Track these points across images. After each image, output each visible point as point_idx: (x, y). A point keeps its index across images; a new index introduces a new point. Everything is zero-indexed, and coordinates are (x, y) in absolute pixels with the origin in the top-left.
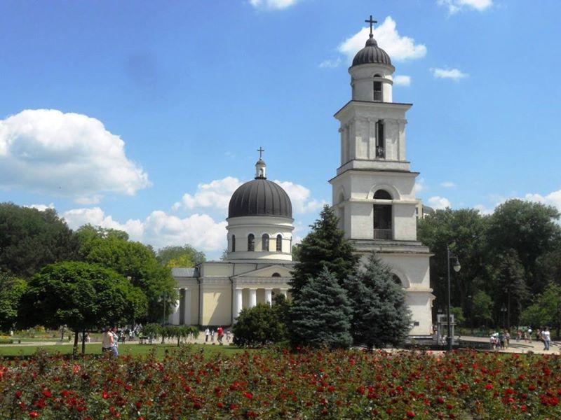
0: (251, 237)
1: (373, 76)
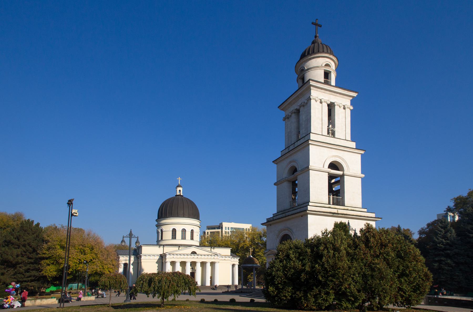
0: (174, 231)
1: (323, 65)
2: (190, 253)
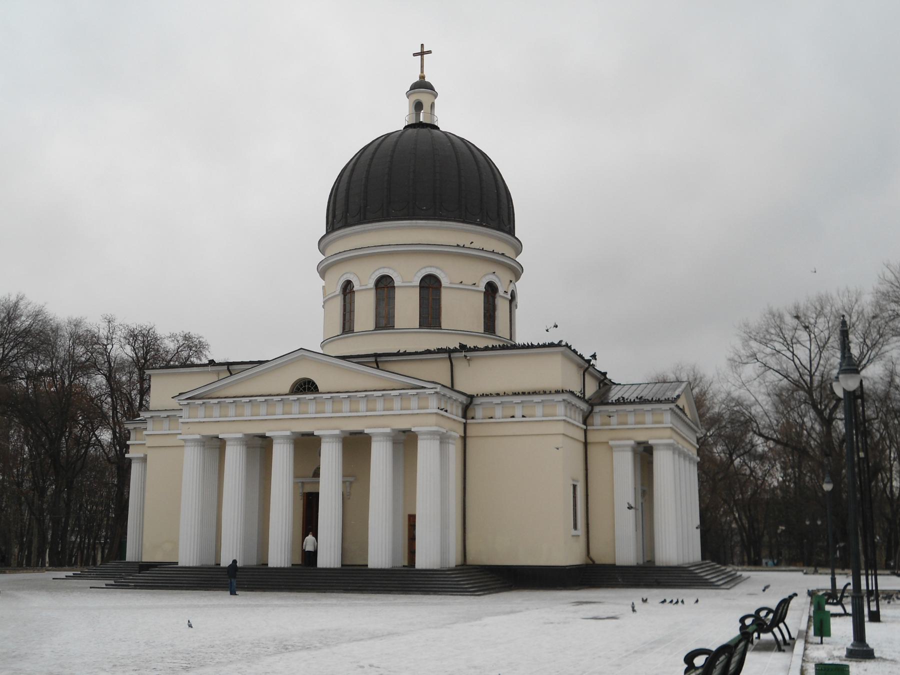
2: (287, 390)
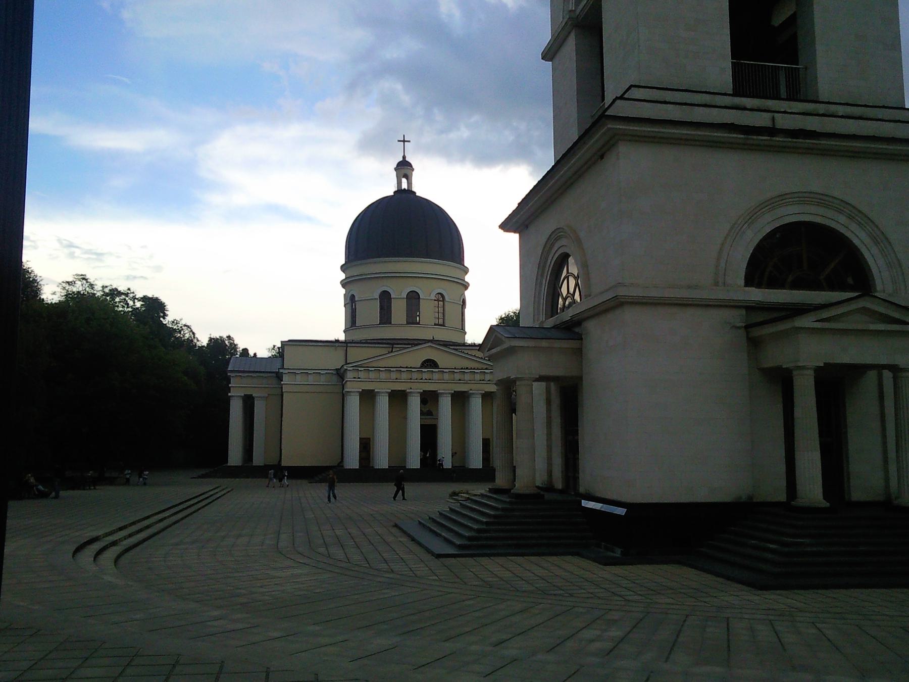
0: (385, 298)
2: (419, 365)
